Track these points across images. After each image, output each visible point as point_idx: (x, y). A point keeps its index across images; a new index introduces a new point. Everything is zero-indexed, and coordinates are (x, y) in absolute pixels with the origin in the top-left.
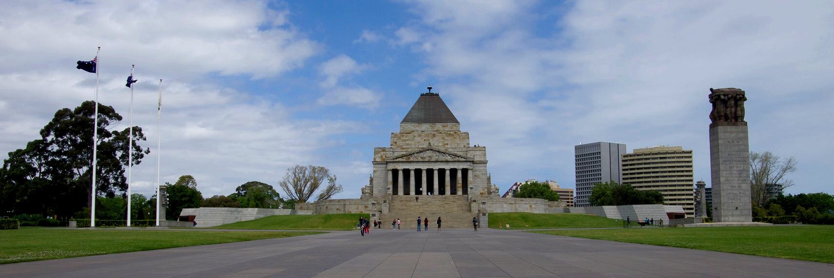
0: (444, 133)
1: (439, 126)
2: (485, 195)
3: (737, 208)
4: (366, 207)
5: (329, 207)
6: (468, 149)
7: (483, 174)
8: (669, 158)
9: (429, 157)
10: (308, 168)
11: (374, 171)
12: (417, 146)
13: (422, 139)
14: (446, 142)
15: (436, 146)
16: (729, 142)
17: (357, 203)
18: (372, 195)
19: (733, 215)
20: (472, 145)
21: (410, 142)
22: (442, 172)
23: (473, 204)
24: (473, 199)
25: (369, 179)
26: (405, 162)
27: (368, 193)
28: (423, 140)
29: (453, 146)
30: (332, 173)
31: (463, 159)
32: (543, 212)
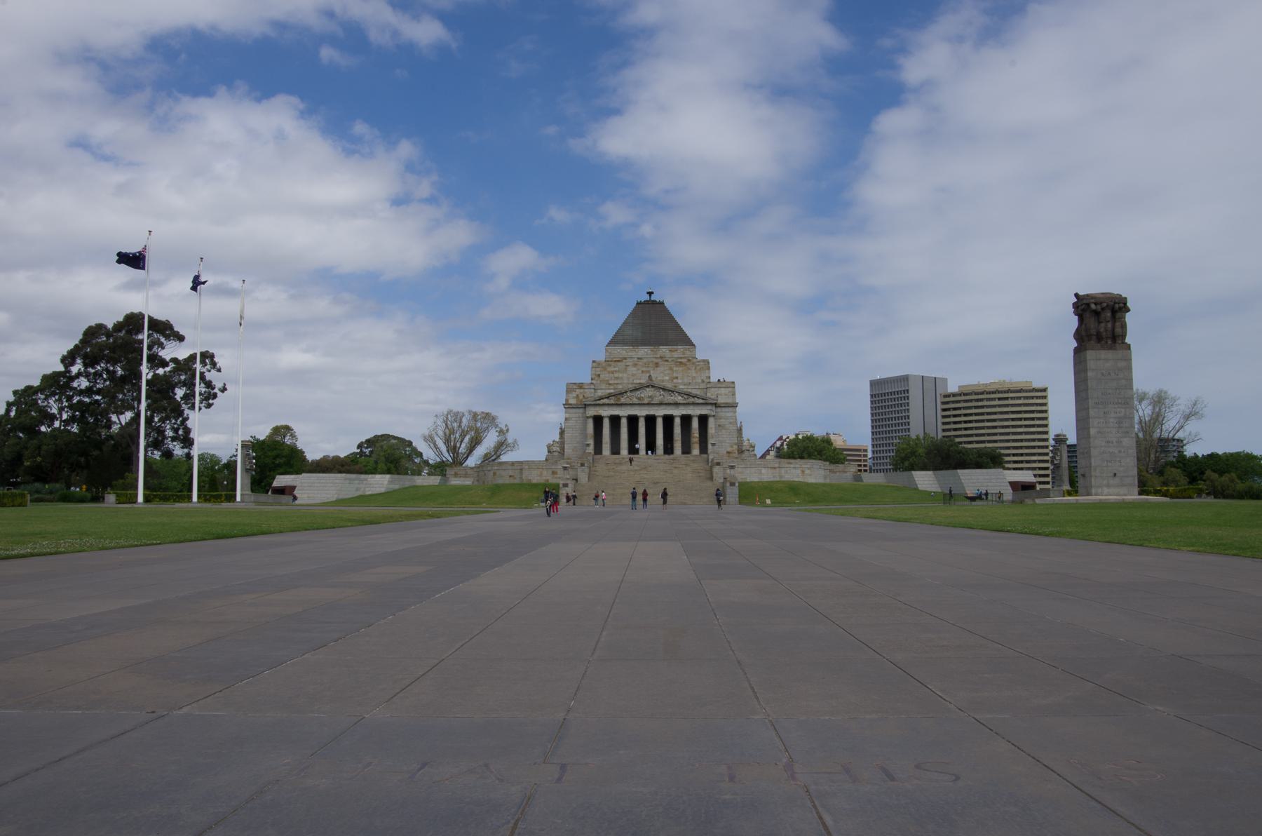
0: (673, 361)
1: (664, 350)
2: (734, 455)
3: (1115, 474)
4: (554, 473)
5: (498, 473)
6: (708, 385)
7: (731, 423)
8: (1012, 398)
9: (650, 397)
10: (466, 414)
11: (566, 419)
12: (631, 381)
13: (639, 370)
14: (675, 375)
15: (660, 380)
16: (1103, 374)
17: (540, 467)
18: (563, 454)
19: (1108, 486)
20: (714, 379)
21: (621, 375)
22: (668, 420)
23: (716, 469)
24: (715, 461)
25: (558, 431)
26: (612, 405)
27: (557, 452)
28: (640, 372)
29: (686, 381)
30: (503, 420)
32: (821, 481)
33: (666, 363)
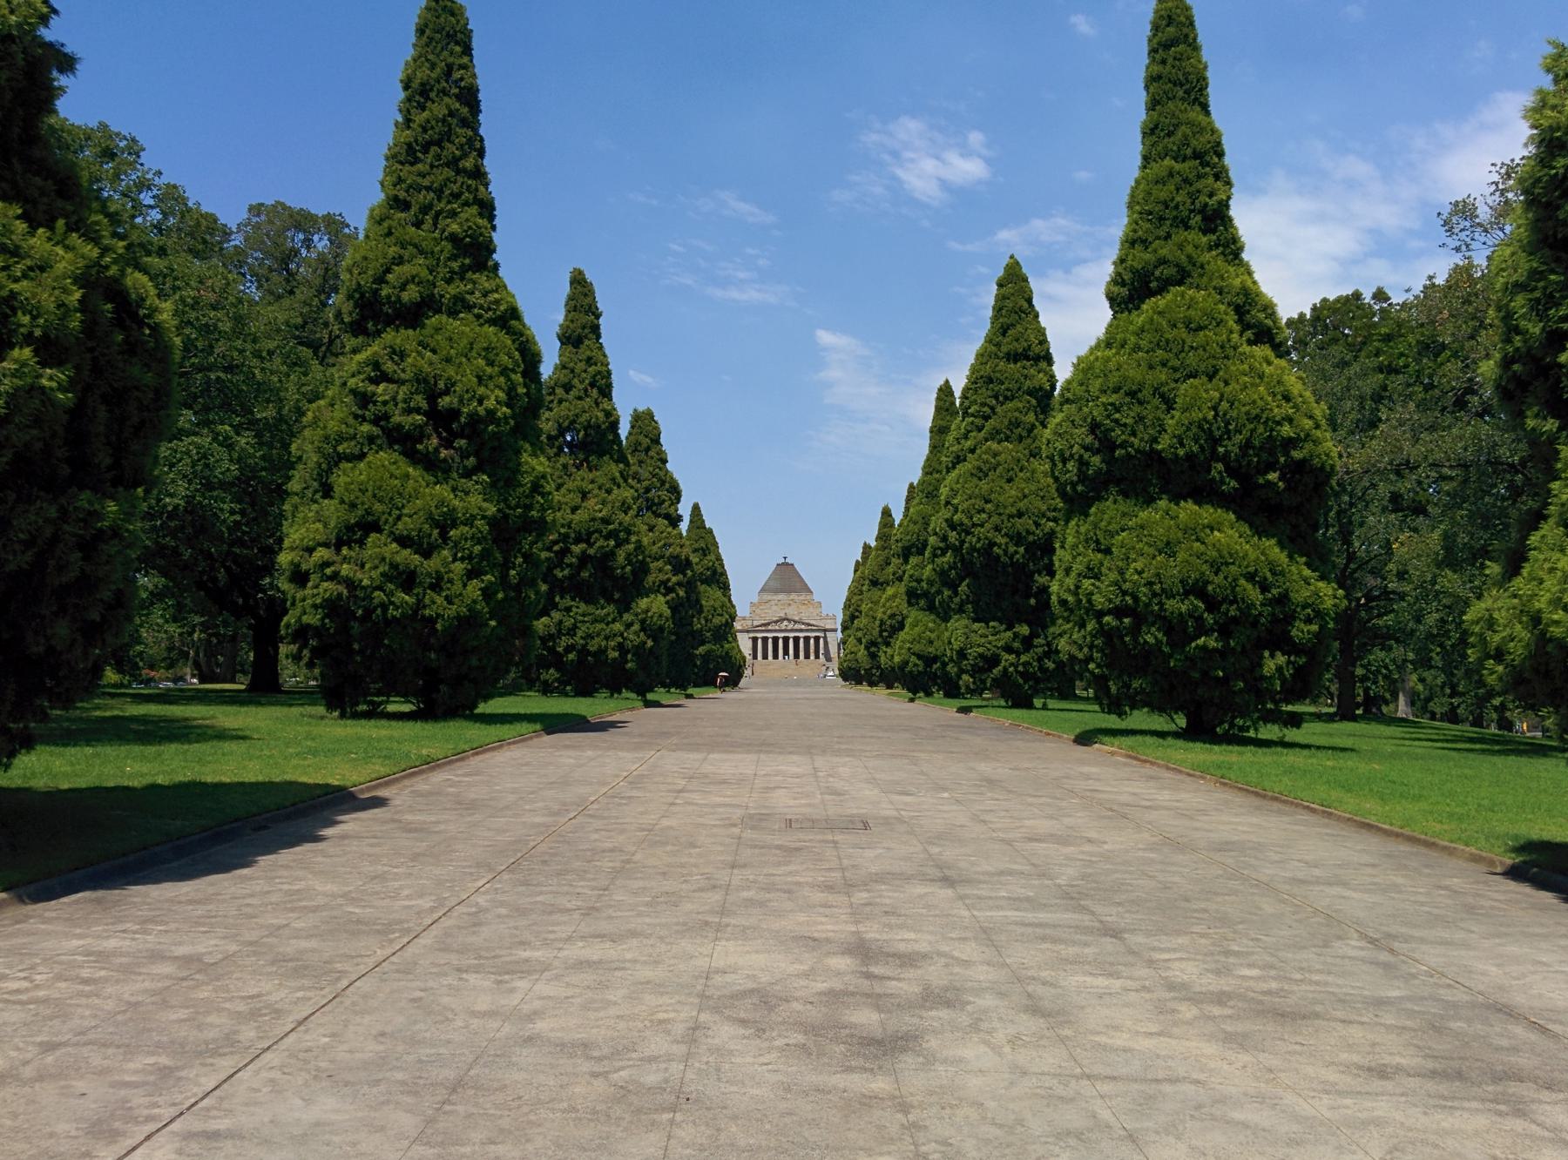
1: (793, 596)
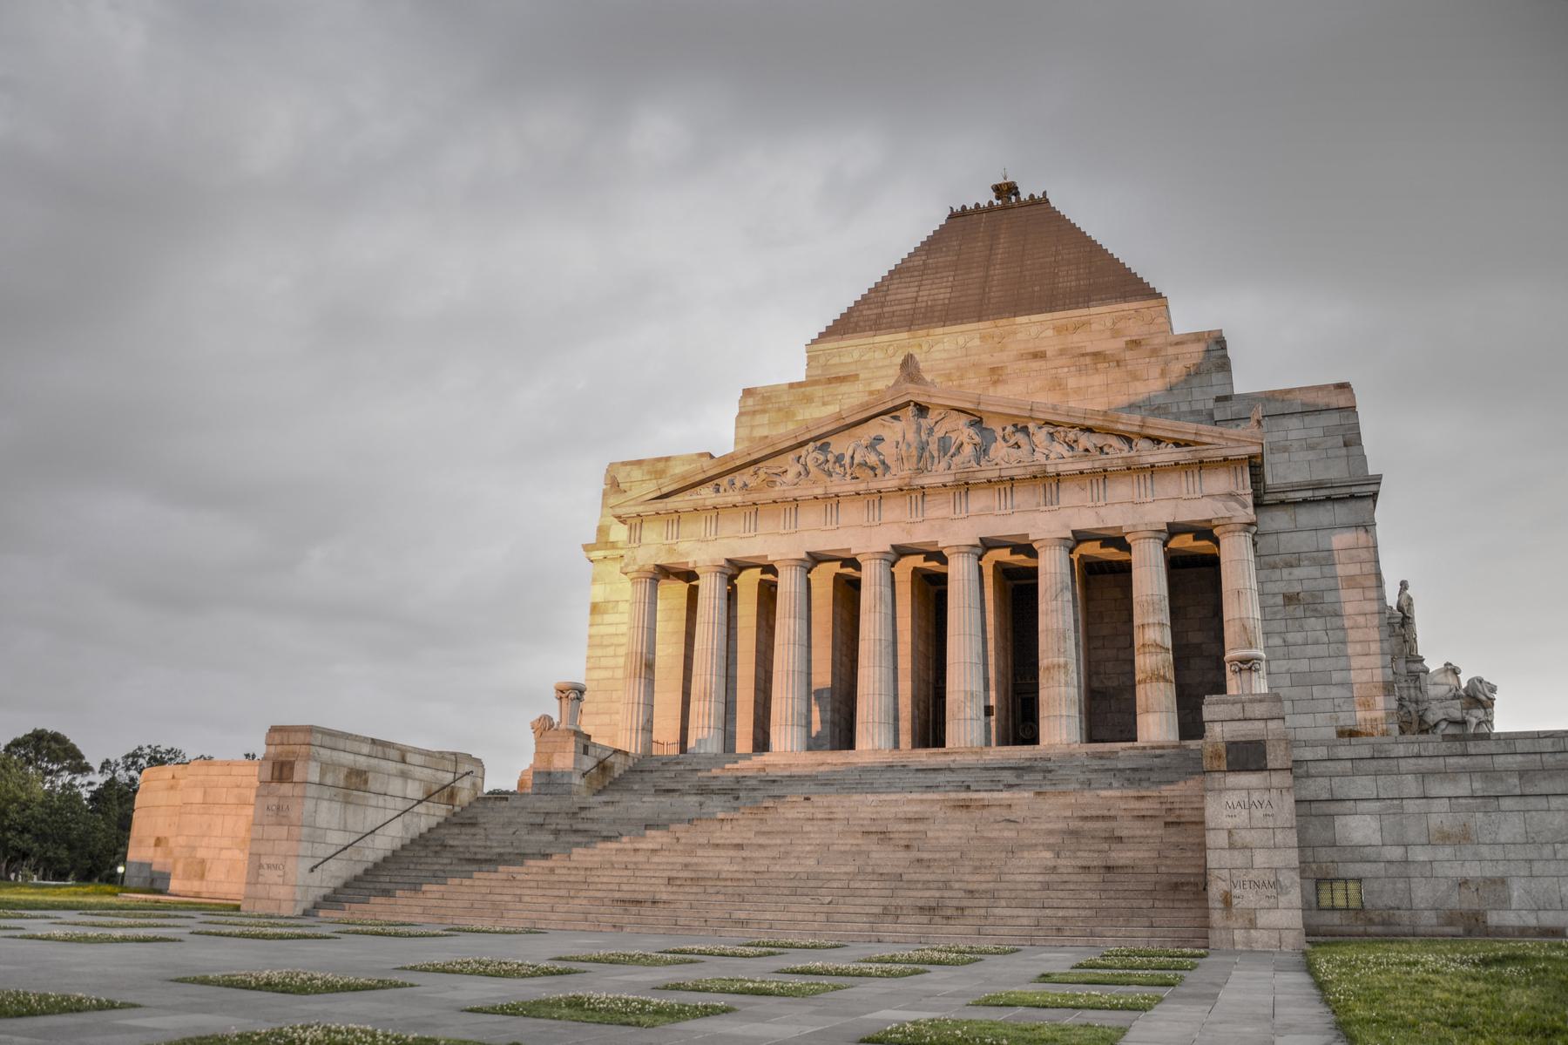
31: (1167, 454)
33: (1036, 364)
